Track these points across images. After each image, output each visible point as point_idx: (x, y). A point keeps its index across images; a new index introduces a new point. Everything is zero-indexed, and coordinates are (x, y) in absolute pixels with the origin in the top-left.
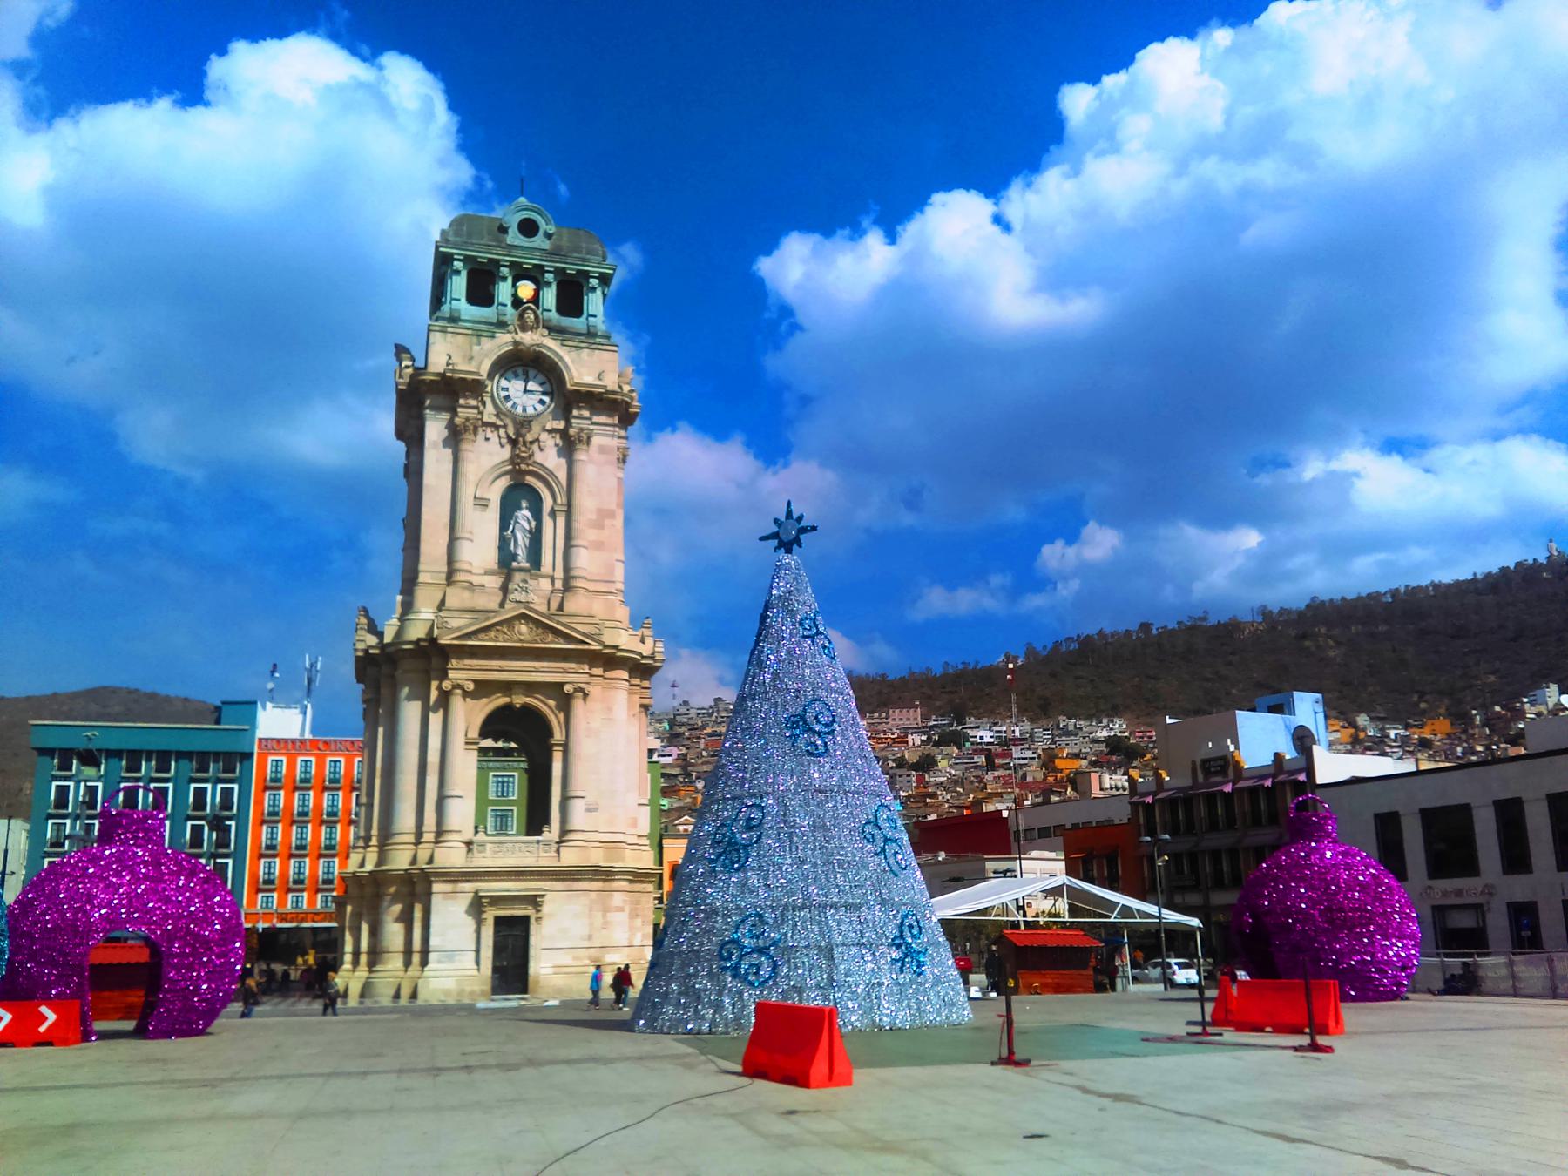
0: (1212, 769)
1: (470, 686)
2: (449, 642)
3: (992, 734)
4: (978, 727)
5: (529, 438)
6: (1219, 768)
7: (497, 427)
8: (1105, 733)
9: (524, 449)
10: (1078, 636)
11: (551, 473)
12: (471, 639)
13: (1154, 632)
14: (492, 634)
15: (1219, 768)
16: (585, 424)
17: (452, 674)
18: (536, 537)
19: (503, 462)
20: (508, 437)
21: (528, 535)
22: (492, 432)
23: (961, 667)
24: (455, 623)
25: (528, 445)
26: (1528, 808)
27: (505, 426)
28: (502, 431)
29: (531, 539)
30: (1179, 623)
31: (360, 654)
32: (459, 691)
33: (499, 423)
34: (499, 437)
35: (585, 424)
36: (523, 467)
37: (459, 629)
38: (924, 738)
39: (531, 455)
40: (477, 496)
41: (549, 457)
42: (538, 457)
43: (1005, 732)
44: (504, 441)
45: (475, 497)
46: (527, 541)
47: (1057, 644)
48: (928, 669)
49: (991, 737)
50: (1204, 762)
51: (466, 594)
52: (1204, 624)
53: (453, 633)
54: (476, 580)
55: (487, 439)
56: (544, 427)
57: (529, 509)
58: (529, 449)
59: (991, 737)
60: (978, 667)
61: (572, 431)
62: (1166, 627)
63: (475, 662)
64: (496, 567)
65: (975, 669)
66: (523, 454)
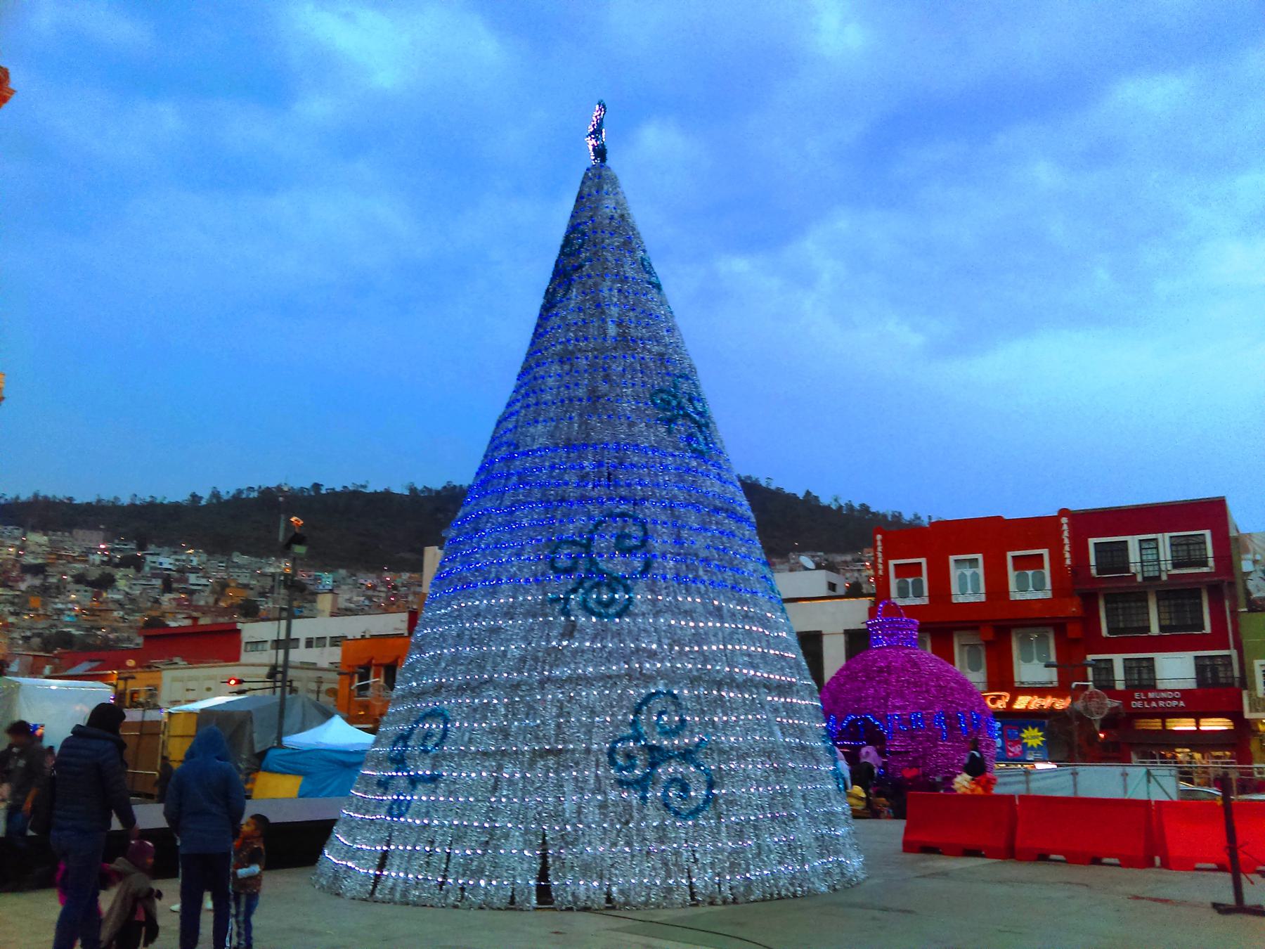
3: (172, 562)
4: (158, 554)
8: (272, 570)
10: (260, 487)
13: (323, 492)
23: (148, 499)
26: (826, 640)
30: (345, 487)
38: (105, 559)
43: (184, 561)
47: (240, 492)
48: (116, 498)
49: (171, 564)
52: (363, 490)
59: (171, 564)
60: (165, 502)
62: (333, 489)
65: (162, 504)
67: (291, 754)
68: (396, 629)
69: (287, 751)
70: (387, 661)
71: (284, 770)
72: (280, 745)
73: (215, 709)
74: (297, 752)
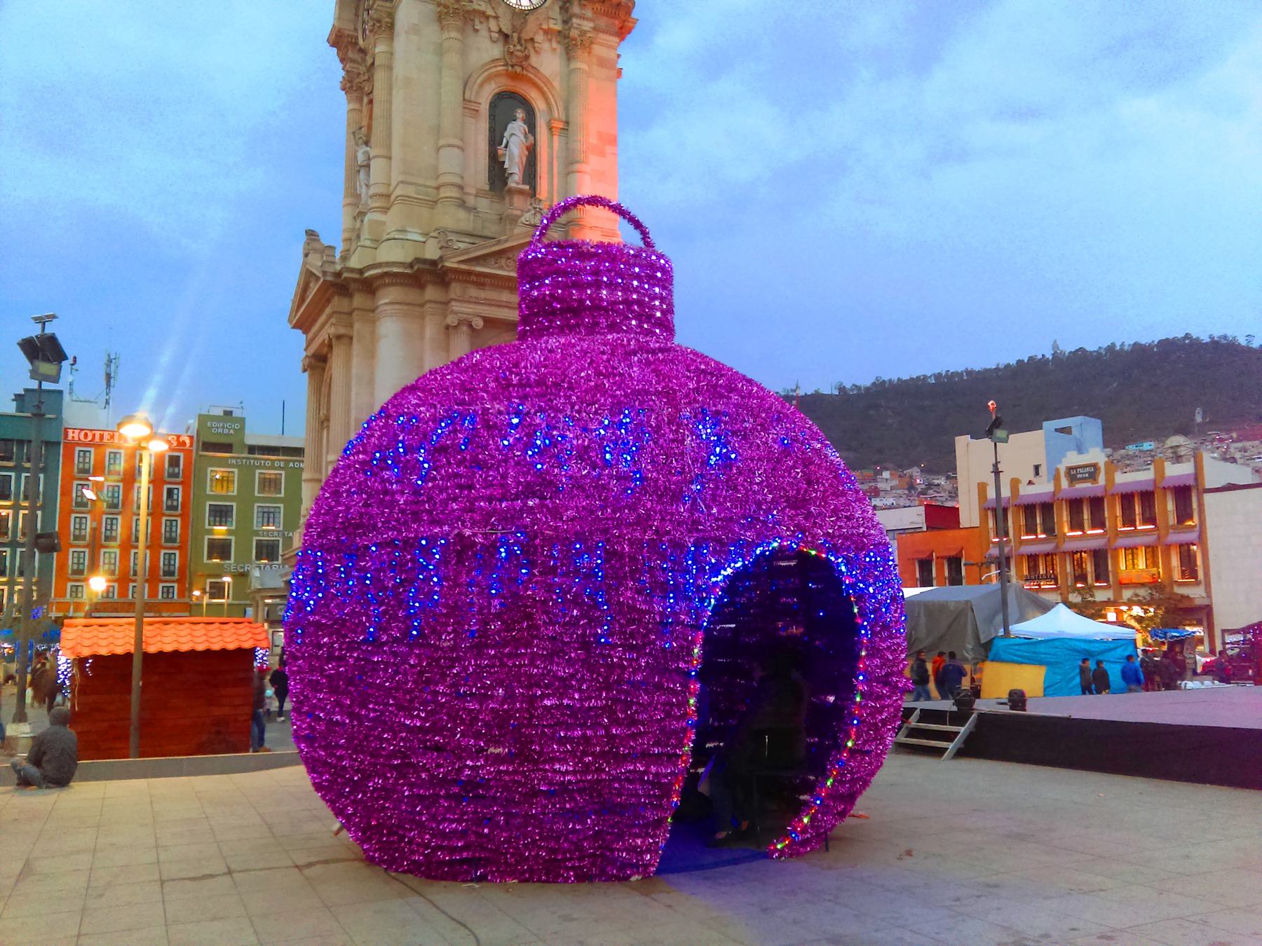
0: (1078, 476)
1: (479, 324)
2: (455, 266)
5: (525, 36)
6: (1087, 475)
7: (488, 17)
9: (519, 47)
11: (547, 82)
12: (479, 264)
14: (503, 261)
15: (1087, 475)
16: (587, 26)
17: (456, 306)
18: (532, 152)
19: (493, 61)
20: (500, 31)
21: (527, 153)
22: (481, 23)
24: (462, 246)
25: (523, 42)
27: (497, 18)
28: (493, 24)
29: (528, 158)
31: (329, 278)
32: (465, 328)
33: (490, 12)
34: (490, 31)
35: (587, 26)
36: (518, 69)
37: (466, 251)
39: (527, 57)
40: (467, 97)
41: (548, 61)
42: (534, 60)
44: (495, 35)
45: (464, 99)
46: (524, 159)
50: (1070, 469)
51: (462, 214)
53: (462, 255)
54: (471, 201)
55: (476, 31)
56: (541, 24)
57: (525, 122)
58: (526, 48)
61: (574, 33)
63: (483, 294)
64: (487, 187)
66: (519, 54)
67: (1027, 644)
68: (912, 523)
69: (1012, 641)
70: (953, 553)
71: (1020, 659)
72: (1007, 632)
73: (912, 599)
74: (1029, 641)
